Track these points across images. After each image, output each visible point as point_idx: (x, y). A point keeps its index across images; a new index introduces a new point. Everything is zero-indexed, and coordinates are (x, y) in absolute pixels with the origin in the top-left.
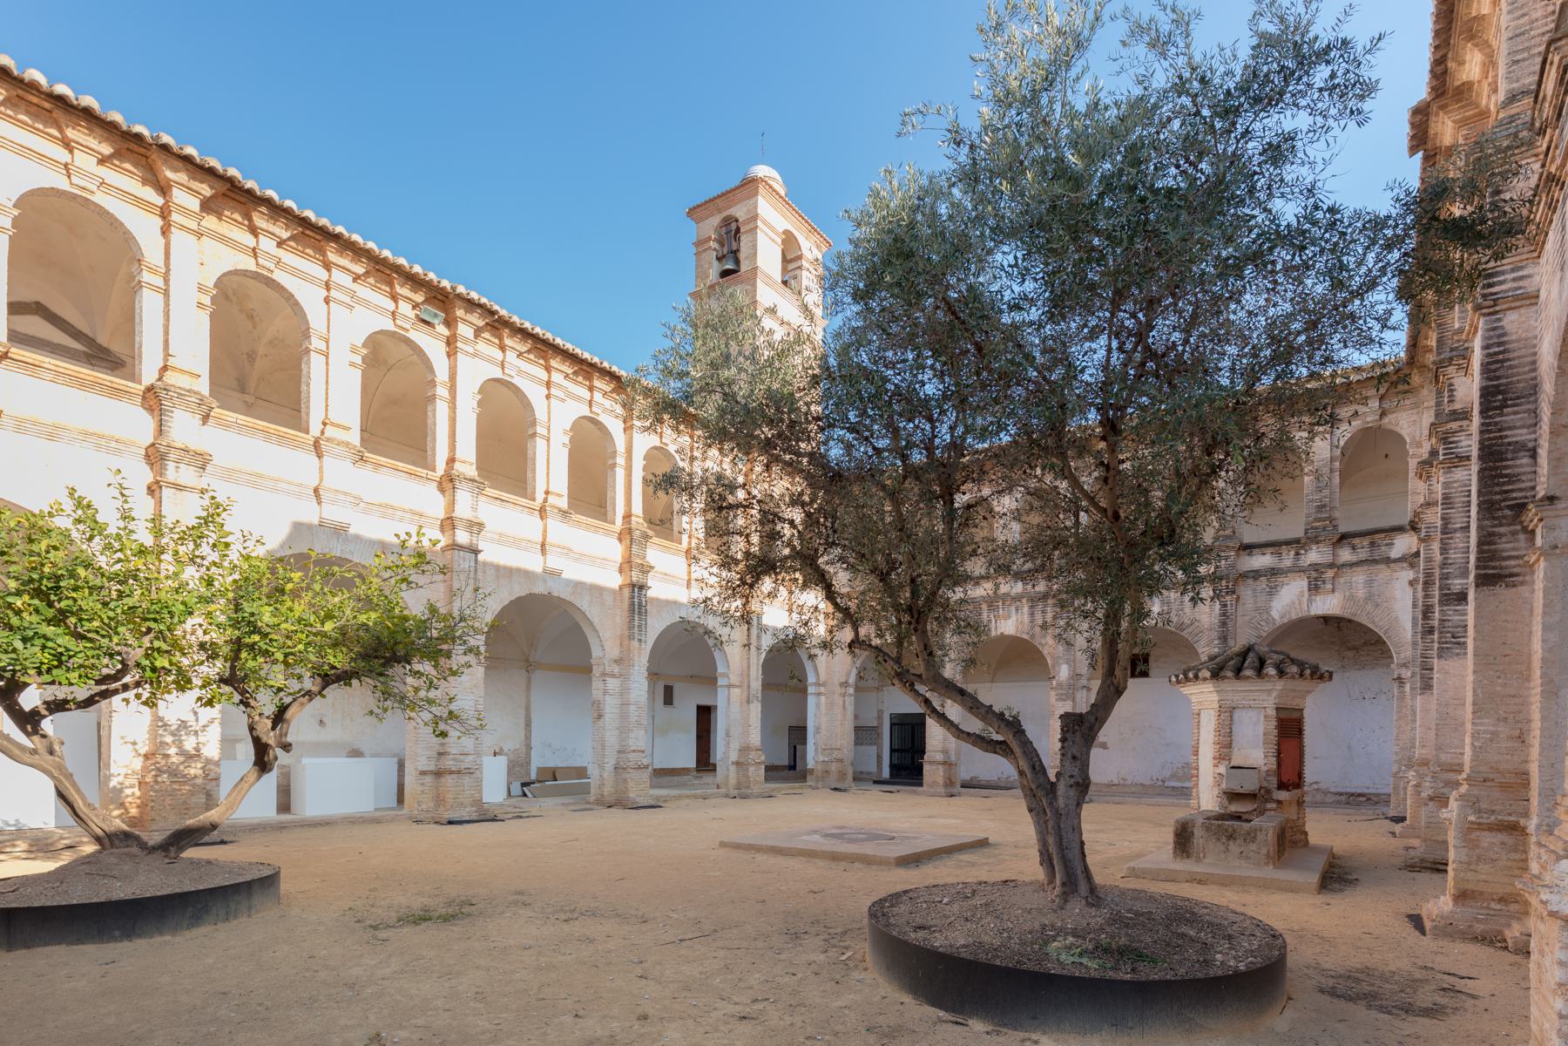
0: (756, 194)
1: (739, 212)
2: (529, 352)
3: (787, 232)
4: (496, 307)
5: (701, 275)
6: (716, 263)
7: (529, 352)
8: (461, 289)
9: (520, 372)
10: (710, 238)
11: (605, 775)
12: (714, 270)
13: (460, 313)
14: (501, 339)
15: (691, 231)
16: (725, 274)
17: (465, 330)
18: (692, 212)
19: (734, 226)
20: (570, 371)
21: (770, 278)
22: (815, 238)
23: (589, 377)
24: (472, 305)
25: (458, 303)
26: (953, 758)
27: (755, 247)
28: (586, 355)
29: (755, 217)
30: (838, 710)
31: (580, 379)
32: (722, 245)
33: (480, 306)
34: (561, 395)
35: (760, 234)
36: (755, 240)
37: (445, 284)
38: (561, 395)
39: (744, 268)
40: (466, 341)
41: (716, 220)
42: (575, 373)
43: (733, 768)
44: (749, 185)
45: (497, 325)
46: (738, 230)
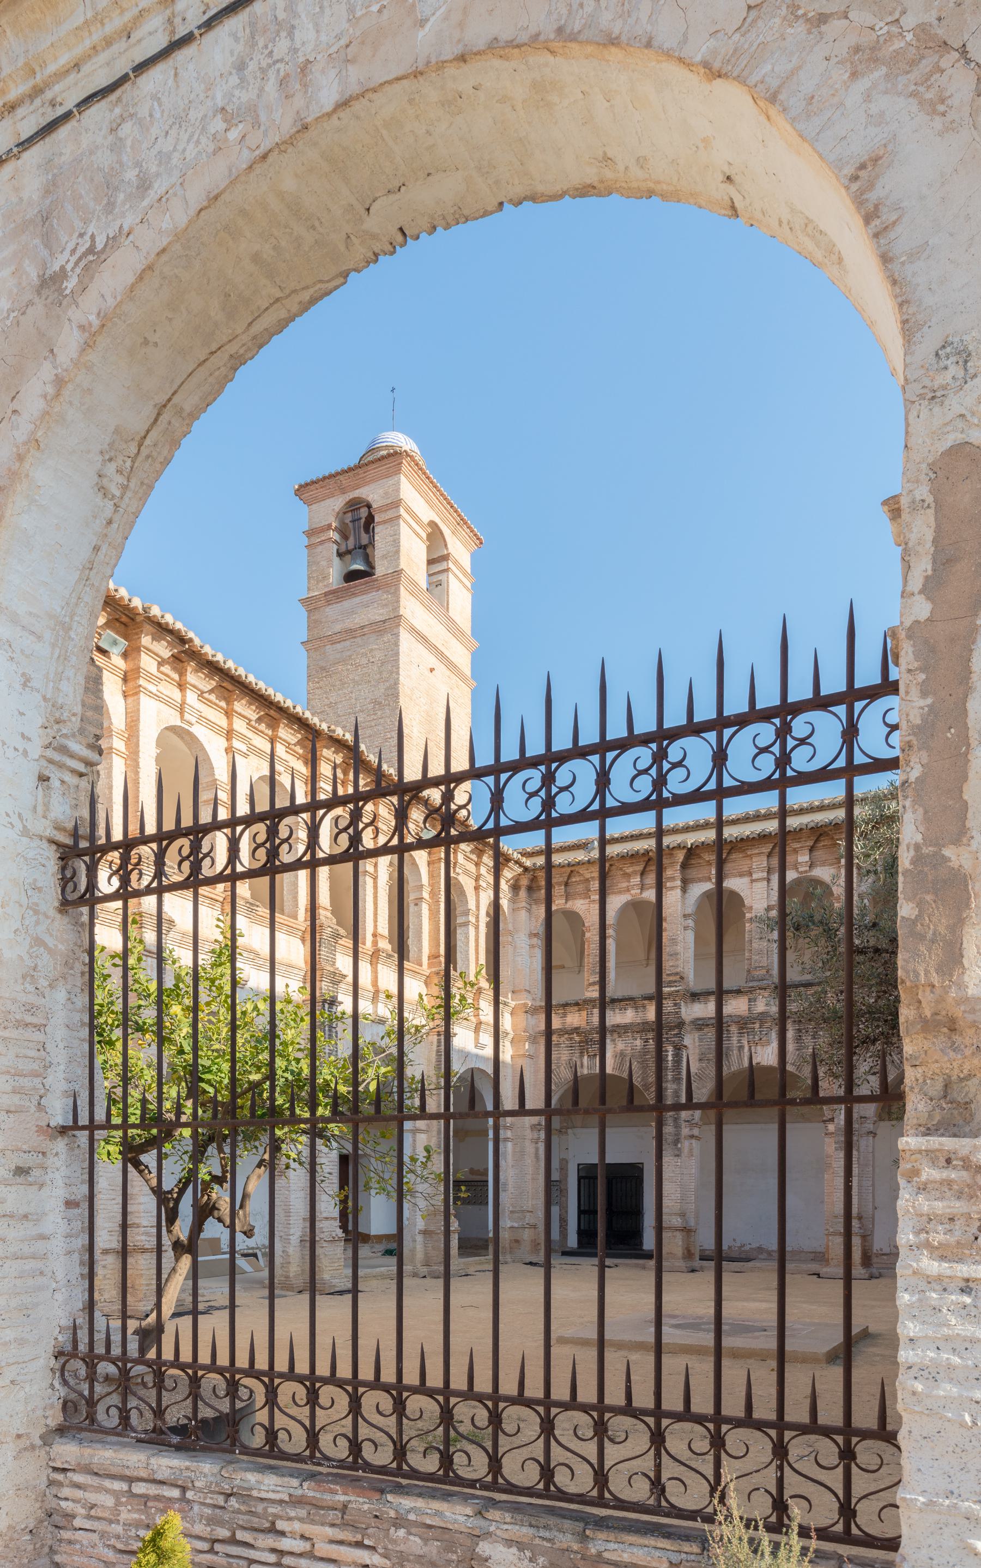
0: (398, 471)
1: (373, 494)
2: (211, 691)
3: (432, 524)
4: (191, 635)
5: (316, 574)
6: (336, 560)
7: (211, 691)
8: (155, 611)
9: (202, 720)
10: (329, 526)
11: (291, 1250)
12: (334, 573)
13: (146, 640)
14: (182, 674)
15: (301, 516)
16: (351, 576)
17: (148, 663)
18: (302, 490)
19: (364, 513)
20: (254, 716)
21: (415, 584)
22: (464, 532)
23: (273, 725)
24: (162, 630)
25: (148, 627)
26: (692, 1223)
27: (396, 543)
28: (279, 698)
29: (397, 504)
30: (529, 1160)
31: (263, 727)
32: (345, 537)
33: (171, 632)
34: (243, 748)
35: (404, 529)
36: (397, 534)
37: (137, 603)
38: (243, 748)
39: (380, 570)
40: (150, 677)
41: (338, 503)
42: (259, 720)
43: (419, 1238)
44: (385, 461)
45: (185, 654)
46: (370, 519)
